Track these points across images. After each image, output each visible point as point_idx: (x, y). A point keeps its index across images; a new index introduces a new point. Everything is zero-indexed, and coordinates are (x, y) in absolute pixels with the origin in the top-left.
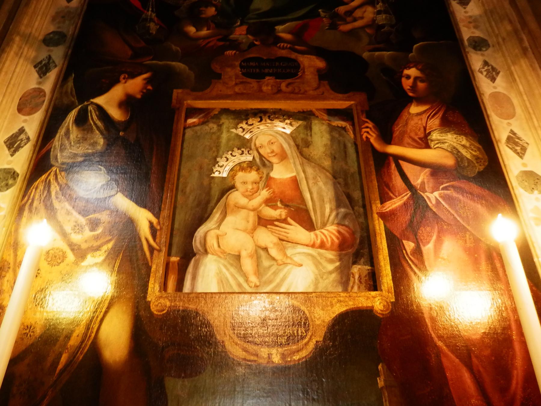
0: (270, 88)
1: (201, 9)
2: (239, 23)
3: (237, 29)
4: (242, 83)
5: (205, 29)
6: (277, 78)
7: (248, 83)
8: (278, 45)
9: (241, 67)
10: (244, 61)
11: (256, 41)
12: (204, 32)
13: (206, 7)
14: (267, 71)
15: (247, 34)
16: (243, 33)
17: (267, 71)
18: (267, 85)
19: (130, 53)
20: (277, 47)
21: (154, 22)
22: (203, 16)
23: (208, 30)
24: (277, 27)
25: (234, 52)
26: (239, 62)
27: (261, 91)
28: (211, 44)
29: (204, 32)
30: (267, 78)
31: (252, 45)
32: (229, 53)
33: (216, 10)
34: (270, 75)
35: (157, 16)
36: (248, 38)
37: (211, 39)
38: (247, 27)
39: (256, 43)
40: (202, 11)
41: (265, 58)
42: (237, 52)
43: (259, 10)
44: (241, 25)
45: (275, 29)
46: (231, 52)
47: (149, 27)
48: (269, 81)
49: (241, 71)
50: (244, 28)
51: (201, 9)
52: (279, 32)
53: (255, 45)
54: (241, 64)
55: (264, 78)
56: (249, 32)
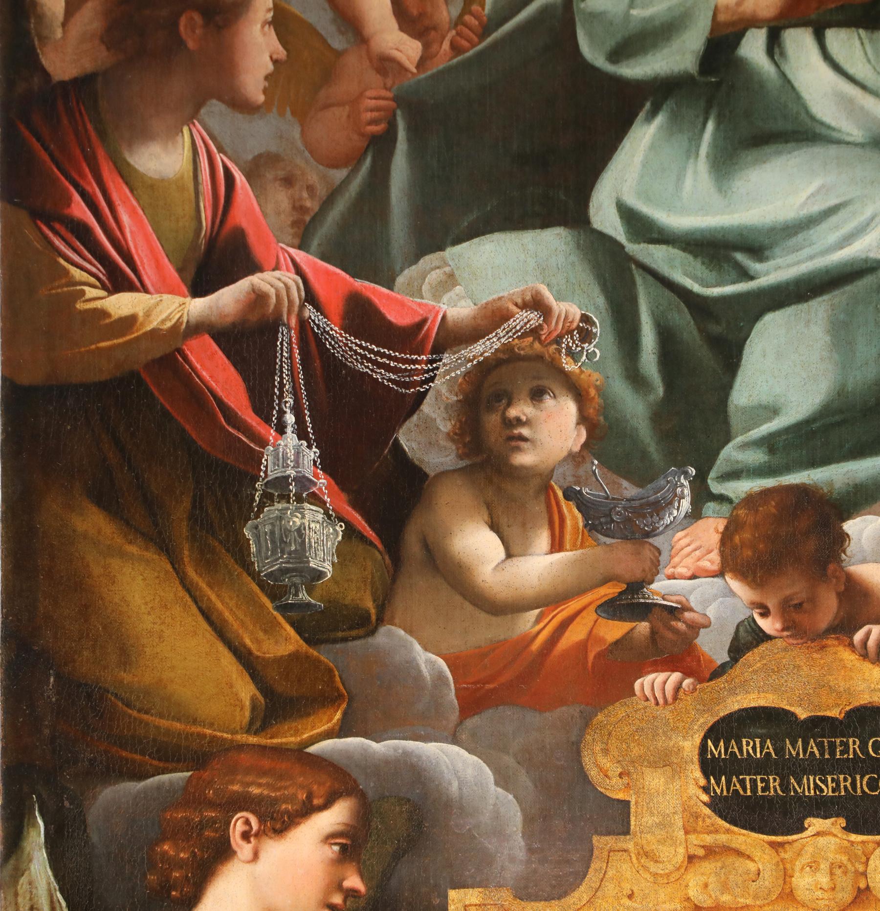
0: (824, 880)
1: (513, 412)
2: (686, 504)
3: (681, 538)
4: (711, 852)
5: (543, 539)
6: (848, 829)
7: (739, 853)
8: (858, 636)
9: (709, 766)
10: (714, 732)
11: (765, 614)
12: (540, 565)
13: (537, 395)
14: (808, 786)
15: (720, 574)
16: (706, 564)
17: (808, 786)
18: (813, 865)
19: (246, 691)
20: (851, 645)
21: (316, 499)
22: (525, 458)
23: (557, 545)
24: (850, 526)
25: (676, 676)
26: (698, 739)
27: (788, 895)
28: (575, 634)
29: (540, 565)
30: (815, 824)
31: (747, 640)
32: (655, 682)
33: (583, 419)
34: (822, 807)
35: (327, 464)
36: (732, 593)
37: (574, 605)
38: (721, 525)
39: (767, 625)
40: (519, 422)
41: (802, 714)
42: (687, 682)
43: (773, 411)
44: (696, 514)
45: (843, 537)
46: (660, 677)
47: (300, 531)
48: (821, 840)
49: (706, 789)
50: (711, 528)
51: (513, 412)
52: (864, 561)
53: (762, 637)
54: (703, 748)
55: (802, 829)
56: (735, 560)
